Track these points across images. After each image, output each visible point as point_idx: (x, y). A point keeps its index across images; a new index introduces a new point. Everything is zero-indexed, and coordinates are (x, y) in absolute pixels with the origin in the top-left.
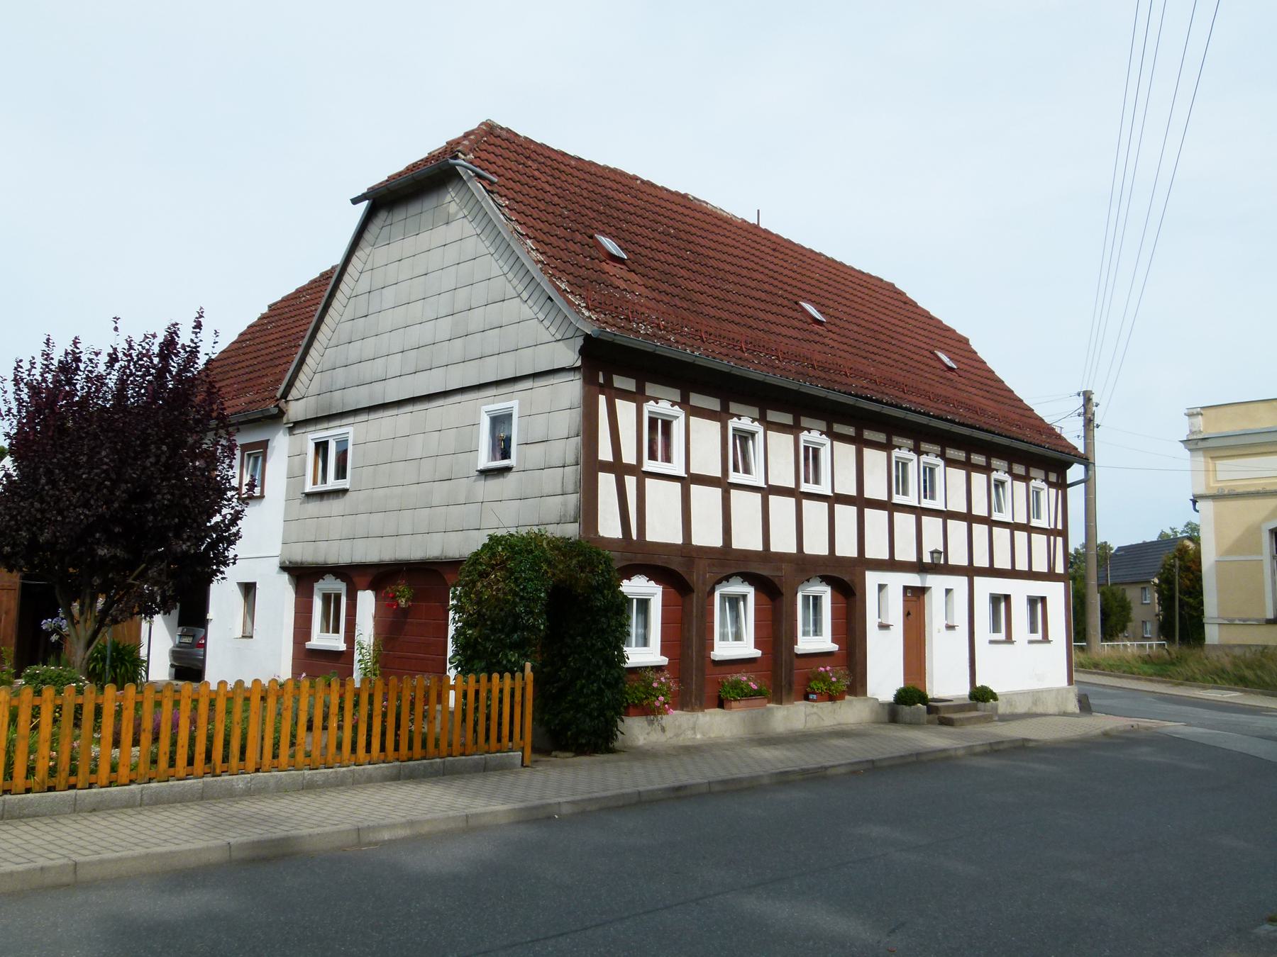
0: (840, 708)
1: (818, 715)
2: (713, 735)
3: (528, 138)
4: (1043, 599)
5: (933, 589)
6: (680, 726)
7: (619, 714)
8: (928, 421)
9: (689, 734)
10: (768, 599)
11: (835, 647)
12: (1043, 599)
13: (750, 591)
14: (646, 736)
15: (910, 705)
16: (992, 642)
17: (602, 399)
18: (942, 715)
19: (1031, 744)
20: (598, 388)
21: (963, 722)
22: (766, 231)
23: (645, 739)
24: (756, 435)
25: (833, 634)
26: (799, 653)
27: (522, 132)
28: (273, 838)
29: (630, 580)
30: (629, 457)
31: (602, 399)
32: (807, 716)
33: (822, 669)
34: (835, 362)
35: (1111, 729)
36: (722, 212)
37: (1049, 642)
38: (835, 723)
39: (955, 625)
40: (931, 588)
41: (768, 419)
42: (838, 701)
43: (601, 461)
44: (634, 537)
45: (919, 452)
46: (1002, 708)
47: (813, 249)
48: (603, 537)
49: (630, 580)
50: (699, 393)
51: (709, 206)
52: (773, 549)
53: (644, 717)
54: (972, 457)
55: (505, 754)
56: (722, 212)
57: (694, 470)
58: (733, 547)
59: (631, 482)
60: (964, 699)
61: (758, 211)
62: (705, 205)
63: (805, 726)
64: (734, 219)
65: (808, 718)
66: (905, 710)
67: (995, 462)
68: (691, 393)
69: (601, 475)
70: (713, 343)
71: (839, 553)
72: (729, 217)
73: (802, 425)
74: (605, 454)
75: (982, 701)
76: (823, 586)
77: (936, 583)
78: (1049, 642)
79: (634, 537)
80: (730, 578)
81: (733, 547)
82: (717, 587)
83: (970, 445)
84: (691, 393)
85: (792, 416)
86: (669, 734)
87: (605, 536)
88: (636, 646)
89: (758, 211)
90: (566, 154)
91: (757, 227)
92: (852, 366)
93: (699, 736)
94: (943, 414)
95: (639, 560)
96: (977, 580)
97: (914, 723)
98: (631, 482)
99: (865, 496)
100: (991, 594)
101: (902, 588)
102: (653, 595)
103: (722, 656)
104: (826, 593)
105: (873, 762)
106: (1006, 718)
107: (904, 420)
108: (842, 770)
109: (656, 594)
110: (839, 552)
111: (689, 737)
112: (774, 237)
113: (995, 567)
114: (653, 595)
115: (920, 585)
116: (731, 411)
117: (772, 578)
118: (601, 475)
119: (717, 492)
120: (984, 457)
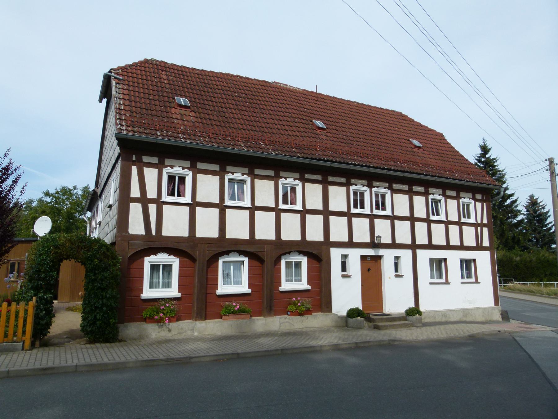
0: (307, 319)
1: (290, 323)
2: (207, 333)
3: (172, 64)
4: (445, 260)
5: (385, 257)
6: (182, 329)
7: (122, 321)
8: (403, 174)
9: (189, 333)
10: (259, 263)
11: (309, 287)
12: (445, 260)
13: (246, 260)
14: (157, 333)
15: (352, 318)
16: (431, 283)
17: (134, 169)
18: (376, 324)
19: (396, 343)
20: (132, 163)
21: (386, 328)
22: (320, 94)
23: (156, 335)
24: (247, 181)
25: (308, 281)
26: (281, 291)
27: (170, 61)
28: (73, 365)
29: (156, 255)
30: (152, 193)
31: (134, 169)
32: (280, 323)
33: (294, 299)
34: (250, 137)
35: (477, 334)
36: (290, 87)
37: (449, 283)
38: (303, 327)
39: (402, 275)
40: (383, 256)
41: (255, 174)
42: (305, 316)
43: (132, 197)
44: (154, 233)
45: (371, 186)
46: (425, 319)
47: (343, 98)
48: (132, 235)
49: (156, 255)
50: (268, 170)
51: (282, 85)
52: (257, 237)
53: (156, 324)
54: (413, 188)
55: (10, 344)
56: (290, 87)
57: (308, 207)
58: (227, 237)
59: (152, 208)
60: (403, 314)
61: (316, 85)
62: (279, 85)
63: (280, 328)
64: (297, 89)
65: (281, 324)
66: (350, 320)
67: (395, 186)
68: (255, 169)
69: (150, 205)
70: (307, 149)
71: (284, 237)
72: (295, 89)
73: (280, 176)
74: (135, 192)
75: (411, 316)
76: (301, 256)
77: (388, 255)
78: (449, 283)
79: (154, 233)
80: (230, 253)
81: (227, 237)
82: (283, 257)
83: (411, 182)
84: (255, 169)
85: (189, 162)
86: (173, 333)
87: (133, 234)
88: (163, 287)
89: (316, 85)
90: (195, 69)
91: (316, 93)
92: (351, 150)
93: (196, 334)
94: (378, 165)
95: (157, 245)
96: (418, 251)
97: (358, 327)
98: (152, 208)
99: (148, 197)
100: (430, 258)
101: (394, 257)
102: (174, 262)
103: (222, 292)
104: (304, 260)
105: (238, 354)
106: (425, 325)
107: (350, 170)
108: (207, 359)
109: (175, 262)
110: (259, 236)
111: (189, 334)
112: (340, 100)
113: (417, 243)
114: (174, 262)
115: (374, 255)
116: (227, 171)
117: (256, 253)
118: (150, 205)
119: (272, 215)
120: (424, 187)
